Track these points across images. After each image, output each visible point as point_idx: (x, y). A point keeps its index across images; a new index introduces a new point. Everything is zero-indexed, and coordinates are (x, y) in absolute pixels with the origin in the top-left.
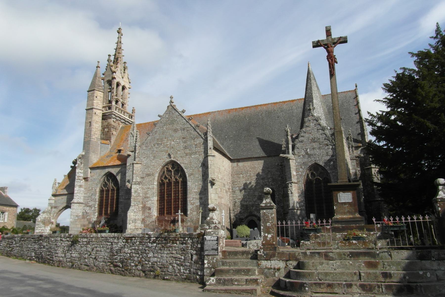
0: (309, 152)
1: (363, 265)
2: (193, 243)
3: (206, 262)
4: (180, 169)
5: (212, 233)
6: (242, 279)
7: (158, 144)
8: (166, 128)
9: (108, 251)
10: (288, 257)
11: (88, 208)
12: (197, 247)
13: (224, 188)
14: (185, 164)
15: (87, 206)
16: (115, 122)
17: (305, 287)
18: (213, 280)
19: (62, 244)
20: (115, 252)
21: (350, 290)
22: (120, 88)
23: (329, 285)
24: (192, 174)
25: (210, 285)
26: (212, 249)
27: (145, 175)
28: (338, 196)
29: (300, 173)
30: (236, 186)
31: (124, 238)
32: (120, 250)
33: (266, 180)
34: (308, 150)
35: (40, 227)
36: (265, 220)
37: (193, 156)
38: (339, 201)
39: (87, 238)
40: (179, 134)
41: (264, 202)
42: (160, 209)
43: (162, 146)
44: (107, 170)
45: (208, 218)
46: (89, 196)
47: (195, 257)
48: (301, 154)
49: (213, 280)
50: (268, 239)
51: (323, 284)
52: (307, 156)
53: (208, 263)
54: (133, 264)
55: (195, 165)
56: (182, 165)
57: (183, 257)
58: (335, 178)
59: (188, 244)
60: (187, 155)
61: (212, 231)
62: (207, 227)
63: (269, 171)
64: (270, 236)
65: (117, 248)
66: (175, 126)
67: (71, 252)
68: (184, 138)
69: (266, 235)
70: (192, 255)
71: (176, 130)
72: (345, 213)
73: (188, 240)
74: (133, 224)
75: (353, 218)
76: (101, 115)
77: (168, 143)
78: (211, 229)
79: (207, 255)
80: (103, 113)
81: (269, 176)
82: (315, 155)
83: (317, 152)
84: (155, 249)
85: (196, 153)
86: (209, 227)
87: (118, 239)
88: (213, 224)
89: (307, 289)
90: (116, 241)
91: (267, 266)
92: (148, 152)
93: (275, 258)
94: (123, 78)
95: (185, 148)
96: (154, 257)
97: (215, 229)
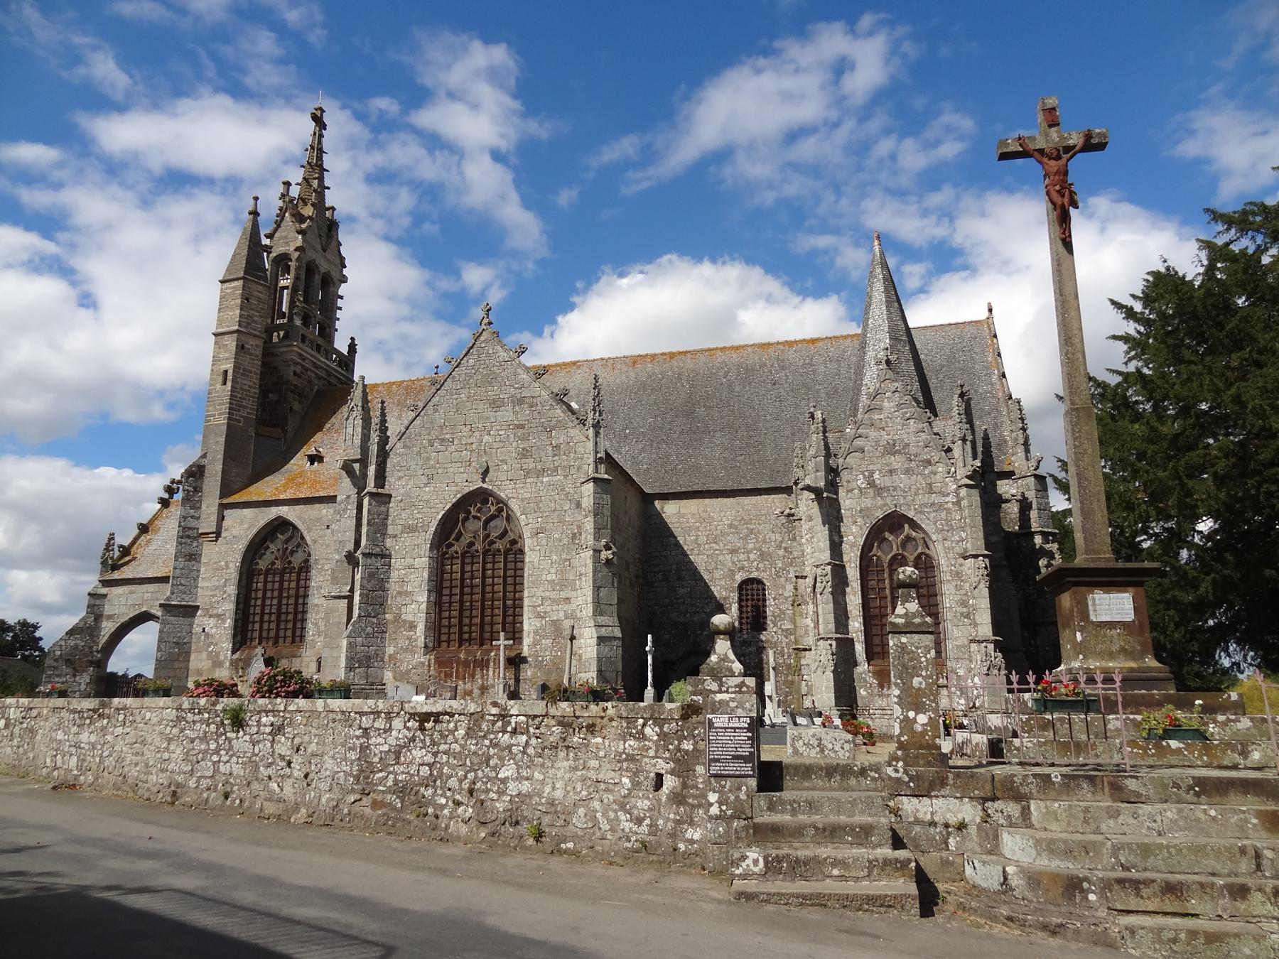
0: (878, 482)
1: (1255, 821)
3: (713, 797)
5: (732, 704)
6: (856, 860)
7: (443, 440)
9: (353, 756)
10: (988, 787)
11: (212, 621)
12: (678, 749)
14: (522, 500)
15: (211, 616)
16: (299, 376)
17: (1085, 893)
18: (756, 862)
19: (182, 730)
21: (1241, 906)
23: (1171, 889)
26: (735, 757)
27: (400, 528)
28: (1090, 603)
30: (657, 569)
31: (412, 716)
34: (876, 476)
35: (59, 676)
36: (905, 667)
38: (1093, 618)
40: (507, 414)
41: (900, 610)
44: (274, 512)
45: (714, 658)
46: (217, 588)
47: (670, 782)
48: (853, 485)
49: (756, 862)
50: (919, 728)
51: (1148, 882)
52: (871, 491)
53: (720, 803)
54: (443, 801)
56: (514, 505)
57: (625, 780)
58: (951, 555)
59: (645, 738)
60: (527, 474)
61: (732, 700)
62: (714, 686)
63: (751, 531)
64: (922, 719)
65: (386, 748)
66: (494, 392)
67: (215, 758)
69: (911, 714)
71: (496, 404)
72: (1111, 656)
73: (644, 725)
75: (1139, 670)
78: (727, 692)
81: (751, 546)
82: (895, 489)
83: (902, 481)
84: (524, 752)
85: (556, 469)
86: (721, 685)
89: (1092, 897)
90: (381, 723)
91: (920, 815)
92: (412, 463)
93: (947, 791)
94: (324, 250)
95: (524, 454)
96: (519, 779)
97: (740, 692)
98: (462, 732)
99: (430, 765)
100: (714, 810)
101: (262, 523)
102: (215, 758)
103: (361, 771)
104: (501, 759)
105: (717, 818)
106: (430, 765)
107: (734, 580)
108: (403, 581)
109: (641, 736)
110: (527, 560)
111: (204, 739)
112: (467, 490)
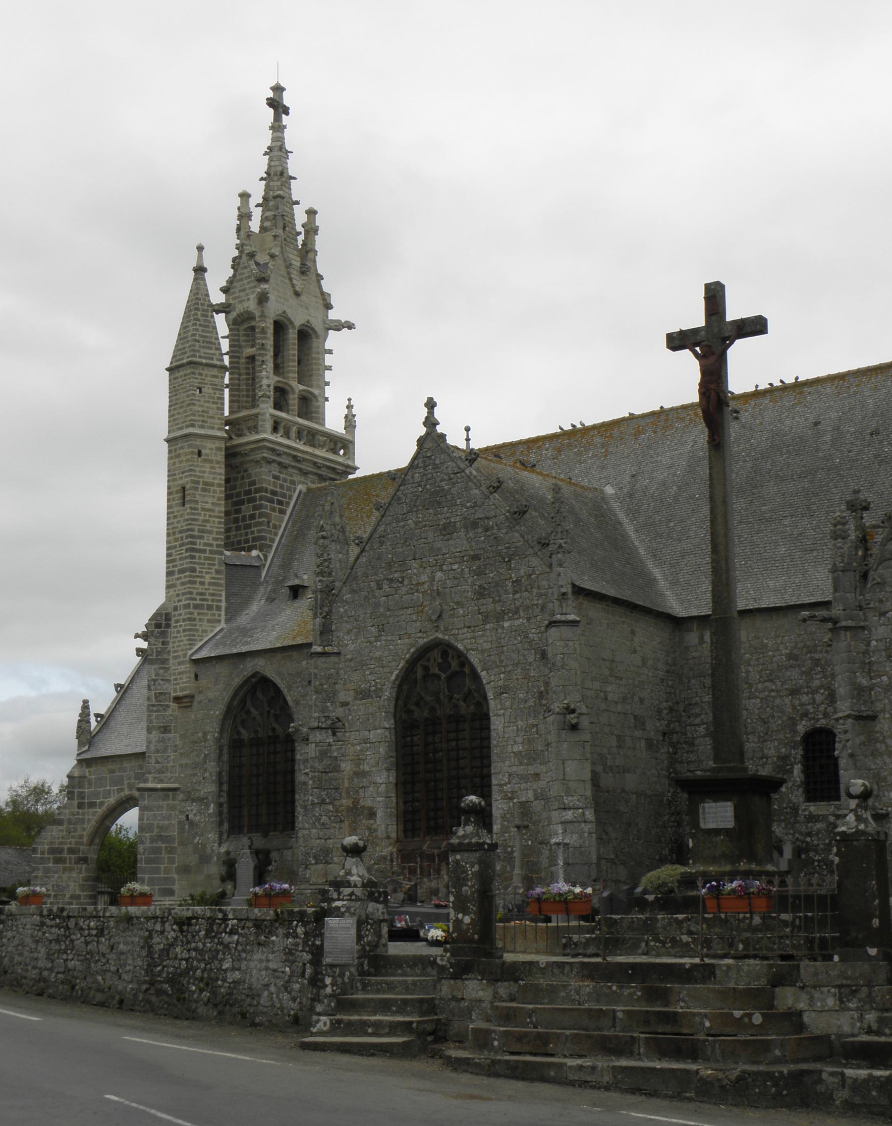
1: (639, 993)
2: (306, 933)
3: (328, 981)
4: (467, 670)
5: (343, 910)
7: (391, 581)
8: (416, 523)
12: (313, 944)
13: (638, 733)
14: (483, 652)
15: (193, 801)
18: (325, 1024)
19: (44, 933)
20: (156, 956)
22: (292, 336)
24: (503, 691)
25: (321, 1033)
28: (701, 811)
29: (885, 678)
30: (698, 721)
32: (168, 951)
33: (805, 698)
37: (506, 624)
38: (703, 826)
39: (97, 917)
40: (461, 542)
42: (405, 812)
43: (404, 590)
44: (250, 667)
47: (309, 971)
53: (333, 985)
54: (194, 988)
55: (514, 656)
56: (475, 659)
57: (287, 969)
60: (486, 619)
63: (816, 662)
64: (467, 920)
67: (65, 957)
68: (475, 557)
69: (460, 916)
70: (304, 964)
71: (447, 530)
72: (714, 860)
73: (297, 926)
74: (320, 866)
76: (221, 457)
77: (424, 578)
78: (343, 900)
79: (332, 966)
80: (227, 449)
81: (817, 683)
85: (517, 612)
87: (163, 923)
88: (350, 887)
90: (158, 927)
95: (481, 593)
96: (233, 969)
97: (350, 900)
98: (203, 933)
99: (187, 960)
100: (329, 990)
101: (237, 681)
102: (65, 957)
103: (149, 965)
104: (224, 954)
105: (331, 996)
106: (187, 960)
107: (795, 732)
108: (358, 760)
109: (296, 936)
110: (492, 727)
111: (58, 941)
112: (422, 642)
